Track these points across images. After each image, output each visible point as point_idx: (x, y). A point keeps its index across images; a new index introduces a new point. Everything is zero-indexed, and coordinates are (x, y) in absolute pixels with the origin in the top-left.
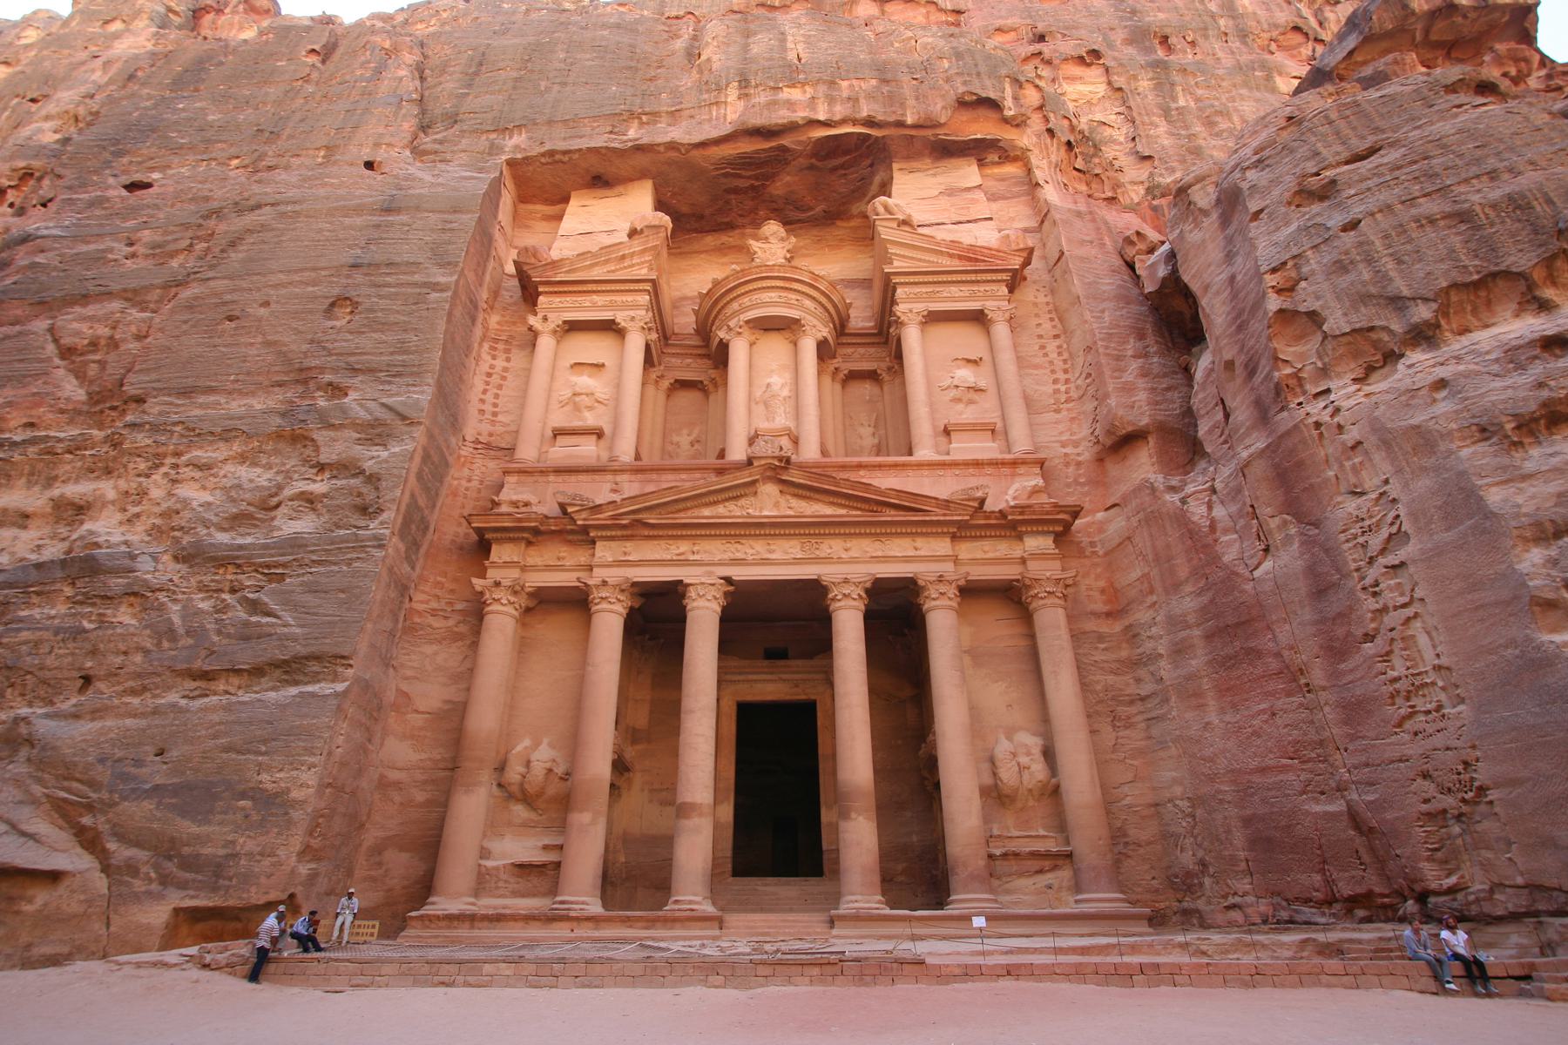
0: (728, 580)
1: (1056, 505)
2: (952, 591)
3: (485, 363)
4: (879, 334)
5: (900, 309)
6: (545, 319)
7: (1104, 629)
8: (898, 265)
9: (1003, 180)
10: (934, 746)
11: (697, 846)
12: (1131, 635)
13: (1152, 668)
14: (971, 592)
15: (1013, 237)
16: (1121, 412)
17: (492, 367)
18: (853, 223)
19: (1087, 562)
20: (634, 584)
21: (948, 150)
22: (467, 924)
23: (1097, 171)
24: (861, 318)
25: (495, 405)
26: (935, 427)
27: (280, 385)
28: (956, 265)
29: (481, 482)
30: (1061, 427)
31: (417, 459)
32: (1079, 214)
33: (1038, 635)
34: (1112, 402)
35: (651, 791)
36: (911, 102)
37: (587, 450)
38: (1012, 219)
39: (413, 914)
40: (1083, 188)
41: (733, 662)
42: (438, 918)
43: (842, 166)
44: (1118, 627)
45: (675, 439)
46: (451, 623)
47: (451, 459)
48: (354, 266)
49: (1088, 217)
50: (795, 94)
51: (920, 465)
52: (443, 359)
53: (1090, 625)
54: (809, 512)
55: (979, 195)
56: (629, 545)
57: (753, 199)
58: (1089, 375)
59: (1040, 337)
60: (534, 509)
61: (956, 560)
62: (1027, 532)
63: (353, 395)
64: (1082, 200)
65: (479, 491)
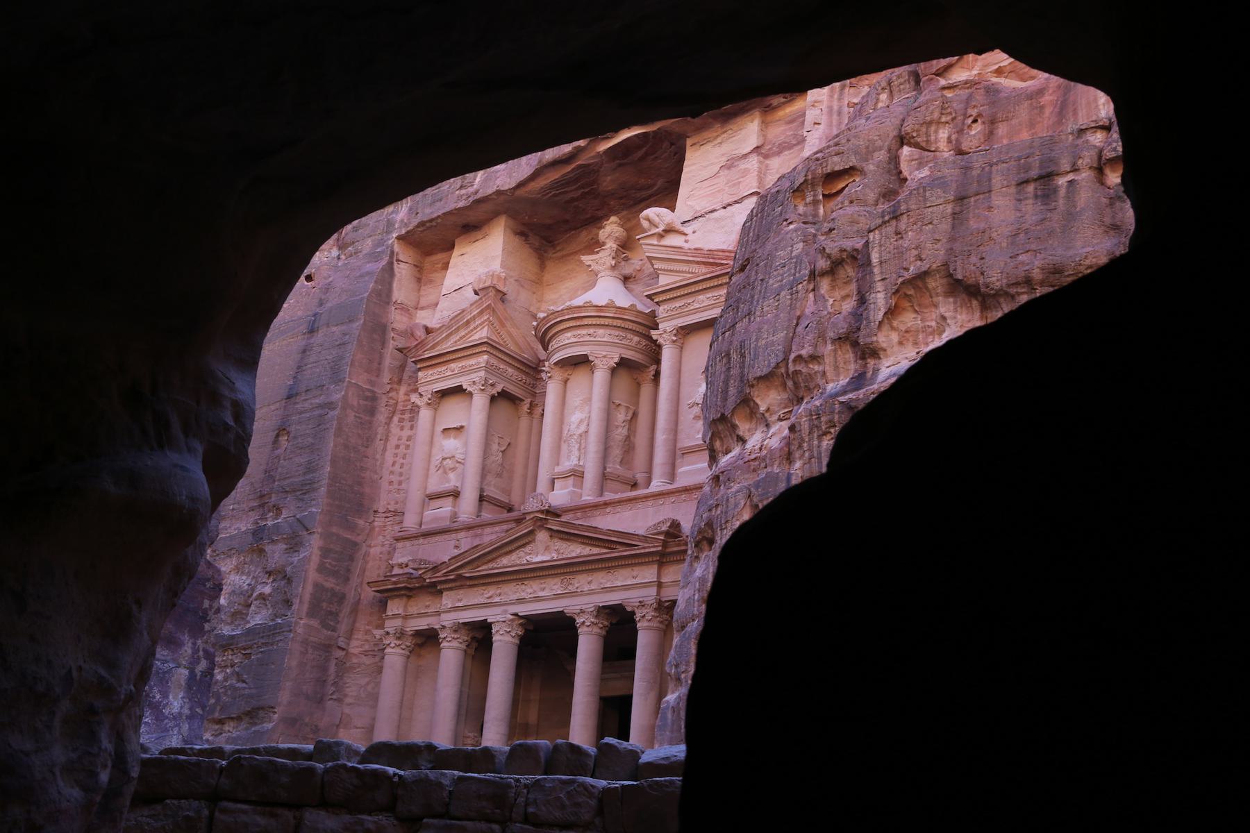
0: (516, 615)
2: (651, 613)
6: (421, 395)
8: (665, 281)
17: (399, 439)
20: (464, 624)
27: (252, 509)
31: (315, 559)
43: (647, 154)
46: (377, 659)
47: (359, 539)
48: (289, 397)
51: (646, 497)
61: (660, 585)
63: (285, 514)
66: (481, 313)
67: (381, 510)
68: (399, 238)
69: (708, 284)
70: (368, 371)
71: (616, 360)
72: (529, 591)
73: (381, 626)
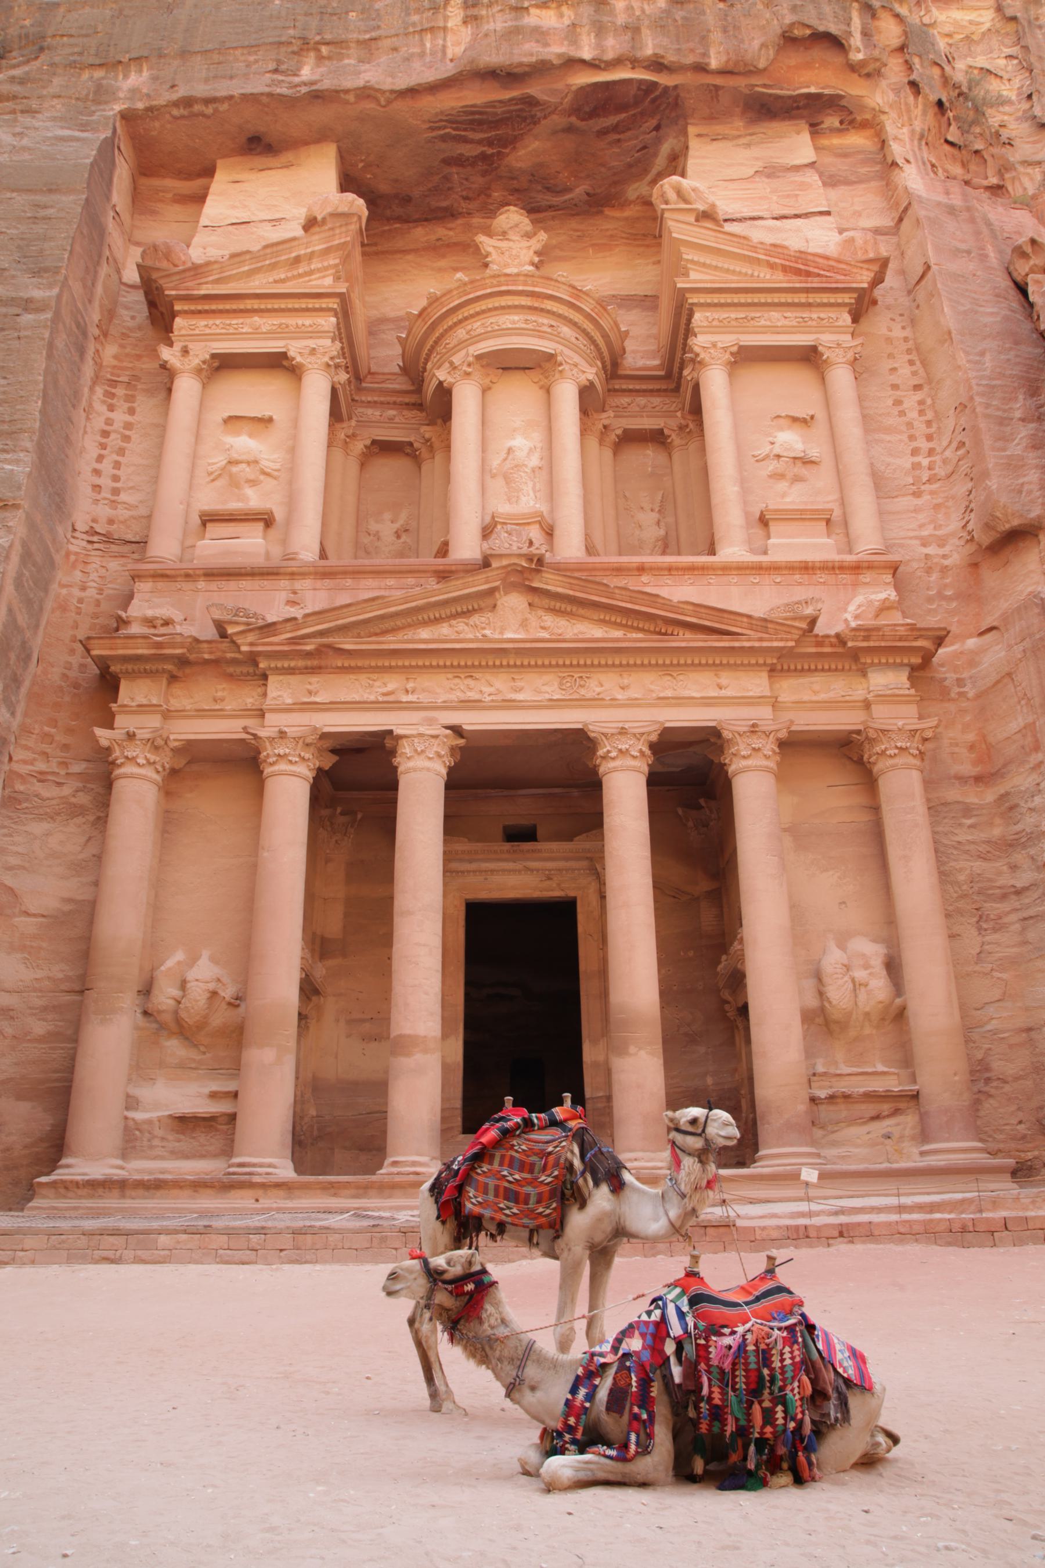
0: (457, 730)
1: (913, 628)
2: (769, 746)
3: (99, 415)
4: (668, 376)
5: (700, 342)
6: (185, 351)
7: (972, 799)
9: (845, 155)
10: (741, 958)
11: (421, 1090)
12: (1008, 807)
13: (1032, 852)
14: (794, 746)
15: (859, 242)
16: (1004, 499)
17: (109, 422)
18: (627, 213)
19: (952, 707)
20: (324, 736)
21: (768, 109)
22: (116, 1192)
23: (979, 145)
24: (642, 353)
25: (116, 478)
26: (747, 514)
28: (780, 280)
29: (100, 591)
30: (922, 517)
31: (15, 559)
32: (951, 211)
33: (885, 808)
34: (993, 483)
35: (350, 1022)
36: (716, 36)
37: (250, 544)
38: (858, 214)
39: (43, 1179)
40: (957, 170)
41: (462, 846)
42: (77, 1184)
43: (615, 128)
44: (990, 796)
45: (373, 527)
46: (66, 791)
47: (58, 558)
49: (965, 215)
50: (547, 19)
51: (727, 569)
52: (43, 412)
53: (953, 794)
54: (569, 635)
55: (812, 177)
56: (315, 681)
57: (484, 174)
58: (962, 444)
59: (895, 387)
60: (179, 629)
62: (872, 664)
64: (956, 188)
65: (98, 603)
66: (327, 252)
67: (81, 526)
68: (127, 117)
69: (789, 298)
70: (85, 286)
71: (591, 377)
72: (492, 690)
73: (110, 726)
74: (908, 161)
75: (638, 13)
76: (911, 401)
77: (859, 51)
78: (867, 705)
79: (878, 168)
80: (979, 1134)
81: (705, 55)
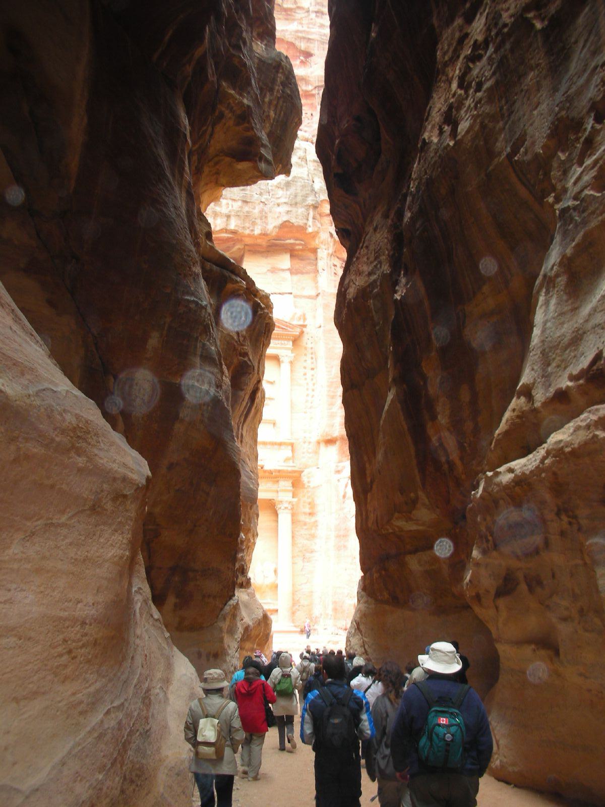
7: (307, 520)
9: (302, 260)
12: (315, 524)
19: (305, 491)
36: (258, 221)
38: (303, 288)
55: (288, 274)
59: (305, 368)
74: (324, 270)
75: (230, 208)
76: (309, 373)
77: (310, 226)
78: (277, 492)
79: (314, 267)
80: (293, 621)
81: (252, 230)
